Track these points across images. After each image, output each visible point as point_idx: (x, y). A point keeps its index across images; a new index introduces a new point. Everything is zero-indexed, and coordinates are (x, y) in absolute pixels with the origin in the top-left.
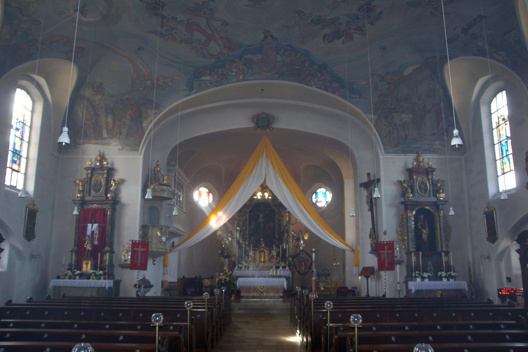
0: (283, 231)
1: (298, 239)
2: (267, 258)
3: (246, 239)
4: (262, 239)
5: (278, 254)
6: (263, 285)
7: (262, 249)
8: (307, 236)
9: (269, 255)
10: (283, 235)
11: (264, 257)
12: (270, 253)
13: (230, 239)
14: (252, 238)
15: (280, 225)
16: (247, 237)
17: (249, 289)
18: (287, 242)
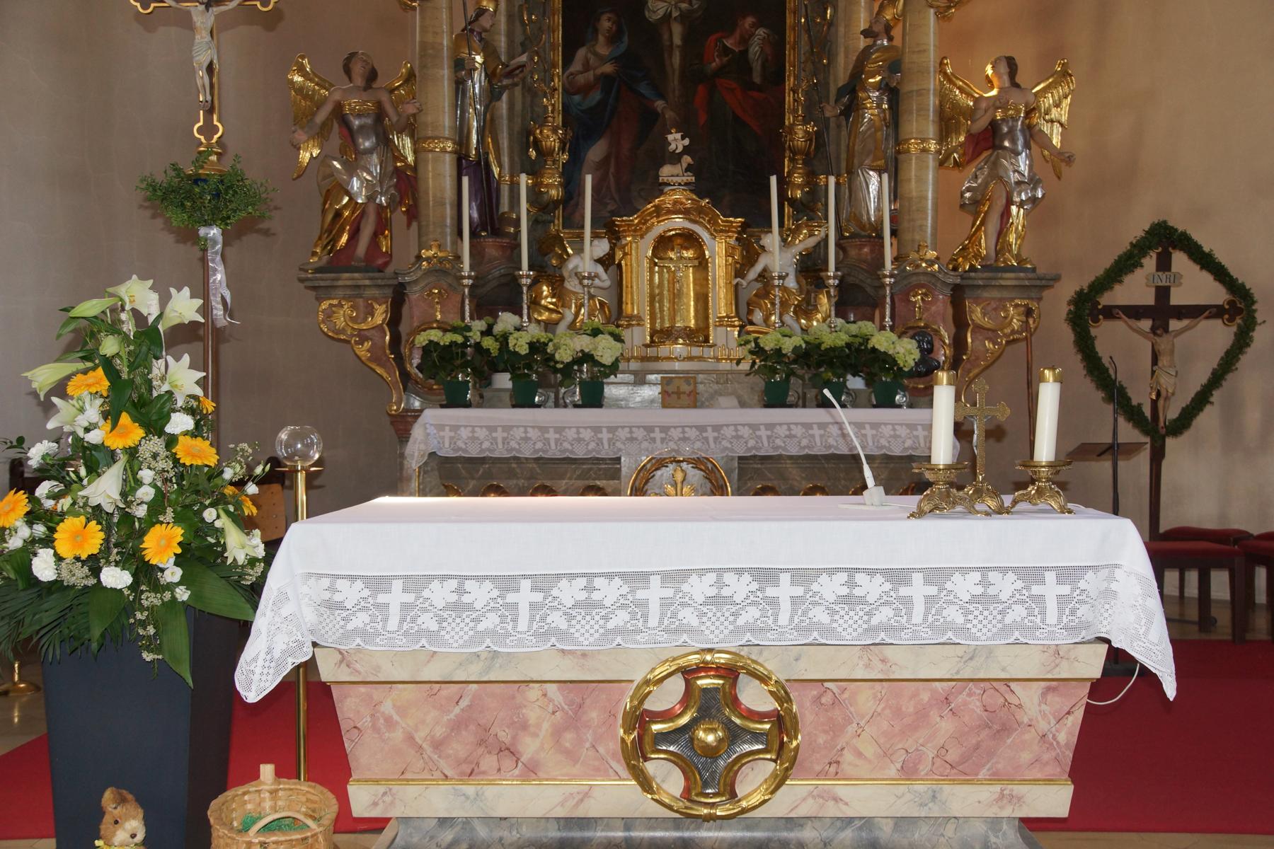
0: (853, 88)
1: (988, 140)
2: (721, 303)
3: (543, 153)
4: (676, 141)
5: (810, 267)
6: (718, 638)
7: (678, 222)
8: (1062, 113)
9: (740, 273)
10: (852, 108)
11: (703, 300)
12: (748, 253)
13: (406, 145)
14: (596, 152)
15: (822, 44)
16: (551, 140)
17: (483, 718)
18: (894, 168)
